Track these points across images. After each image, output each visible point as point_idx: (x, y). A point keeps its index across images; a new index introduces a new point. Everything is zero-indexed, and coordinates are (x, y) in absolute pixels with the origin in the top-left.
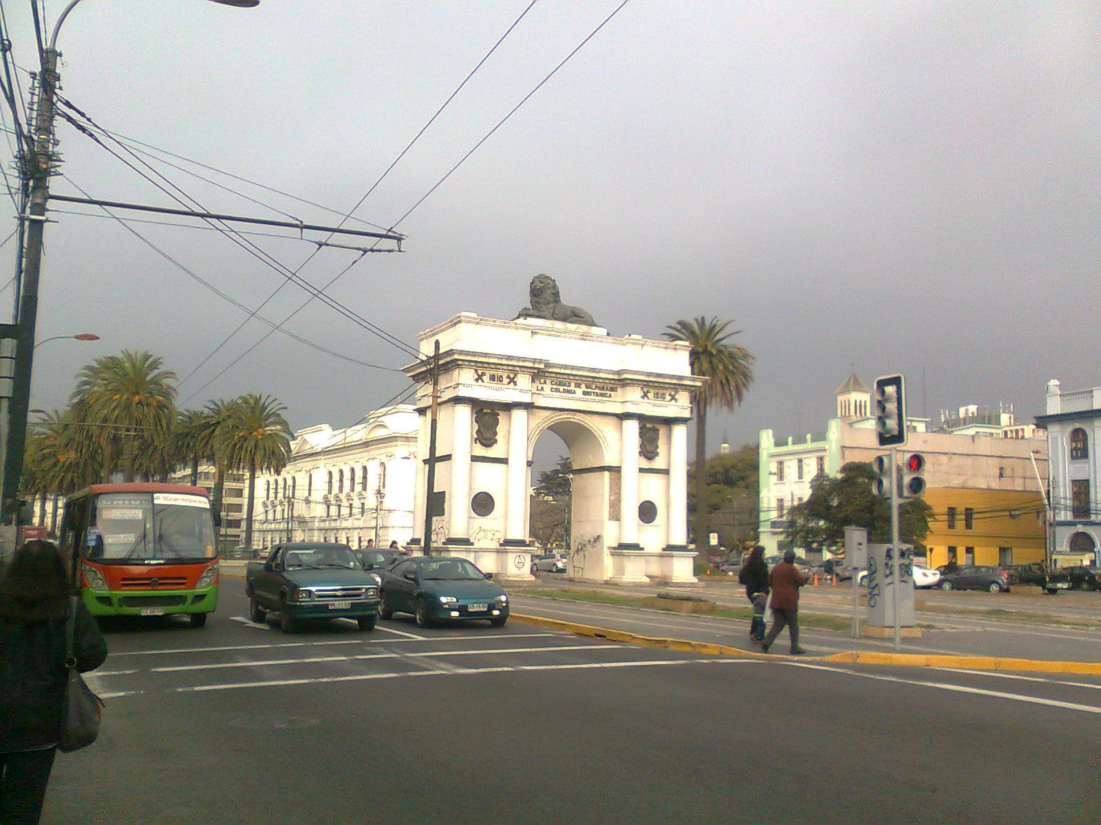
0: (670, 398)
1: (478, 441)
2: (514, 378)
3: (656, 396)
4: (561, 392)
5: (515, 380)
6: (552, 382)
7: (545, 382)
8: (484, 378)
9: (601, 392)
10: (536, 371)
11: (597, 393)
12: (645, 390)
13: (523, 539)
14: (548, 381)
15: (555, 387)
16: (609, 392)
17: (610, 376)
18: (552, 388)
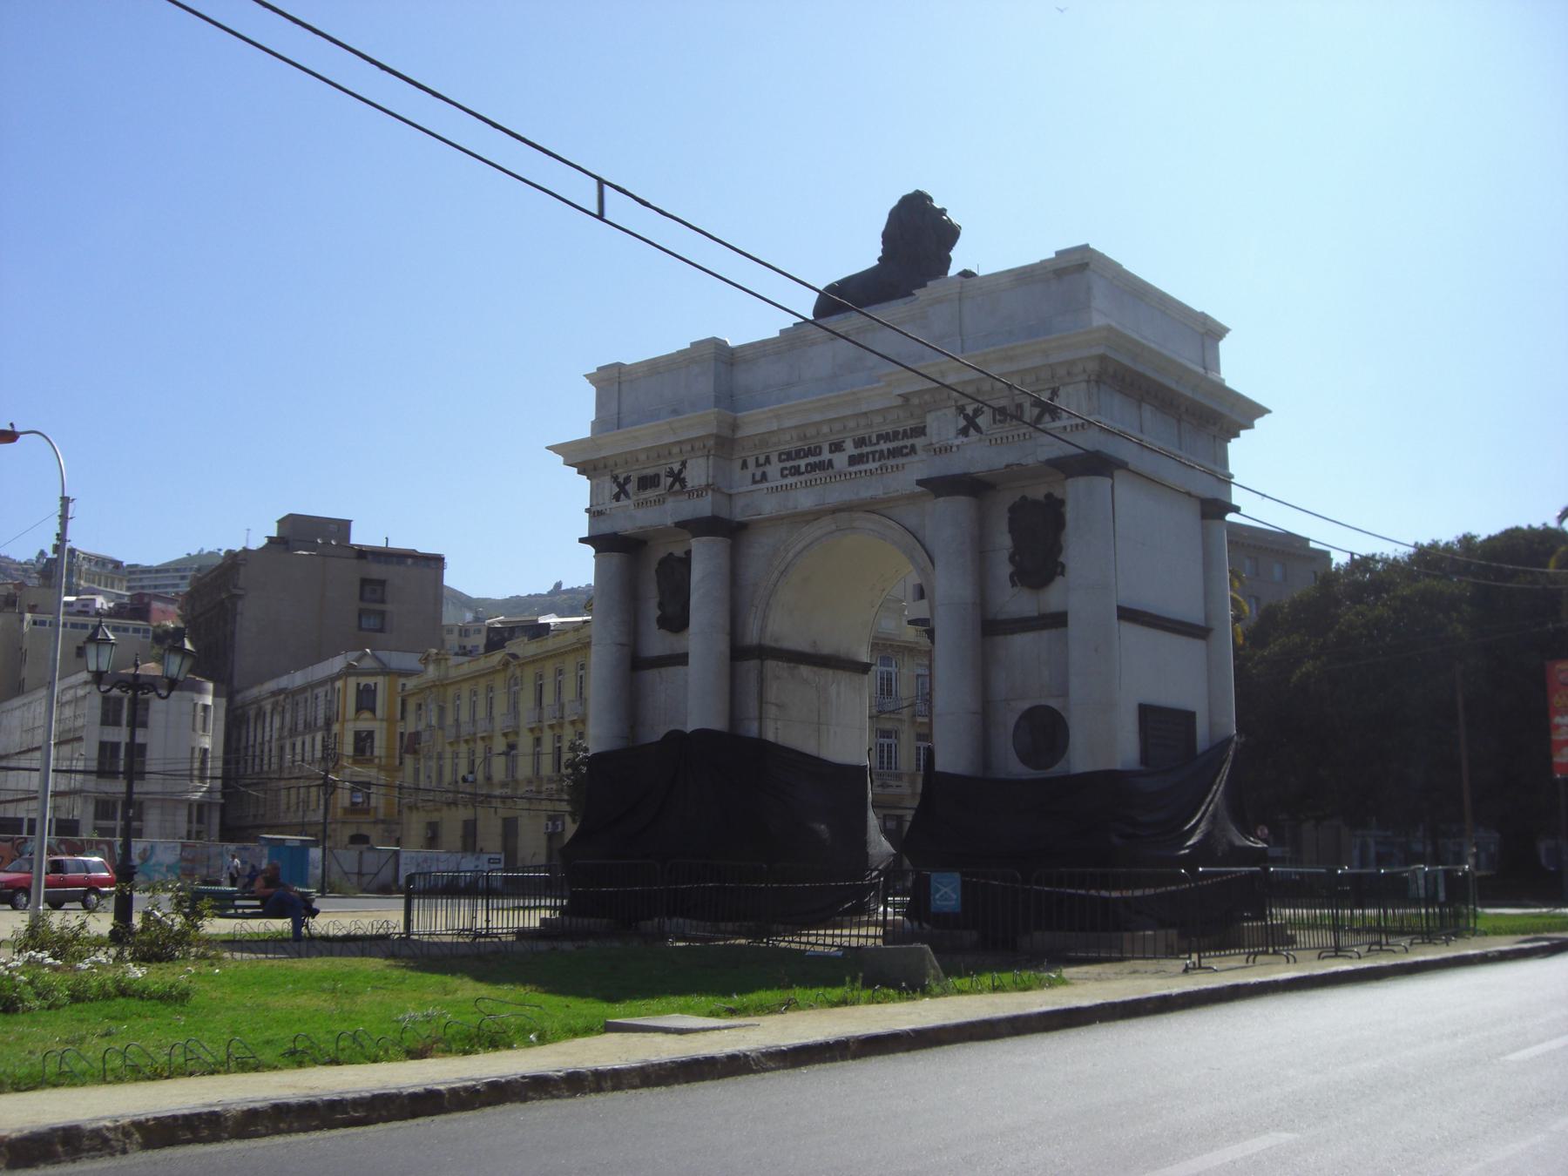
2: (680, 471)
4: (803, 473)
5: (682, 476)
6: (780, 455)
7: (768, 460)
9: (891, 445)
11: (882, 451)
15: (789, 464)
16: (908, 442)
18: (783, 469)
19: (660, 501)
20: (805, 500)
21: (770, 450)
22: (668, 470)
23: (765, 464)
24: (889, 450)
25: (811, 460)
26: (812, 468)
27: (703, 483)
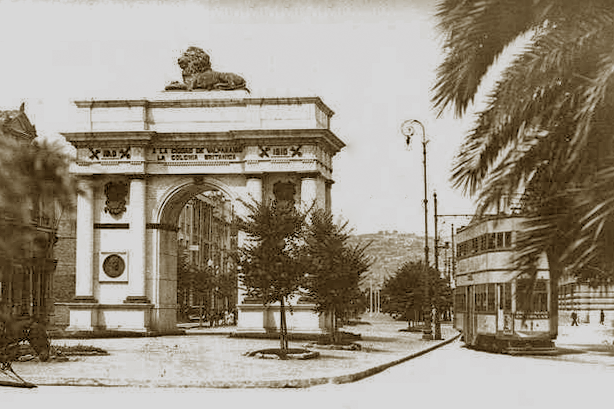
0: (292, 152)
3: (277, 152)
7: (166, 152)
8: (100, 155)
14: (169, 151)
17: (226, 139)
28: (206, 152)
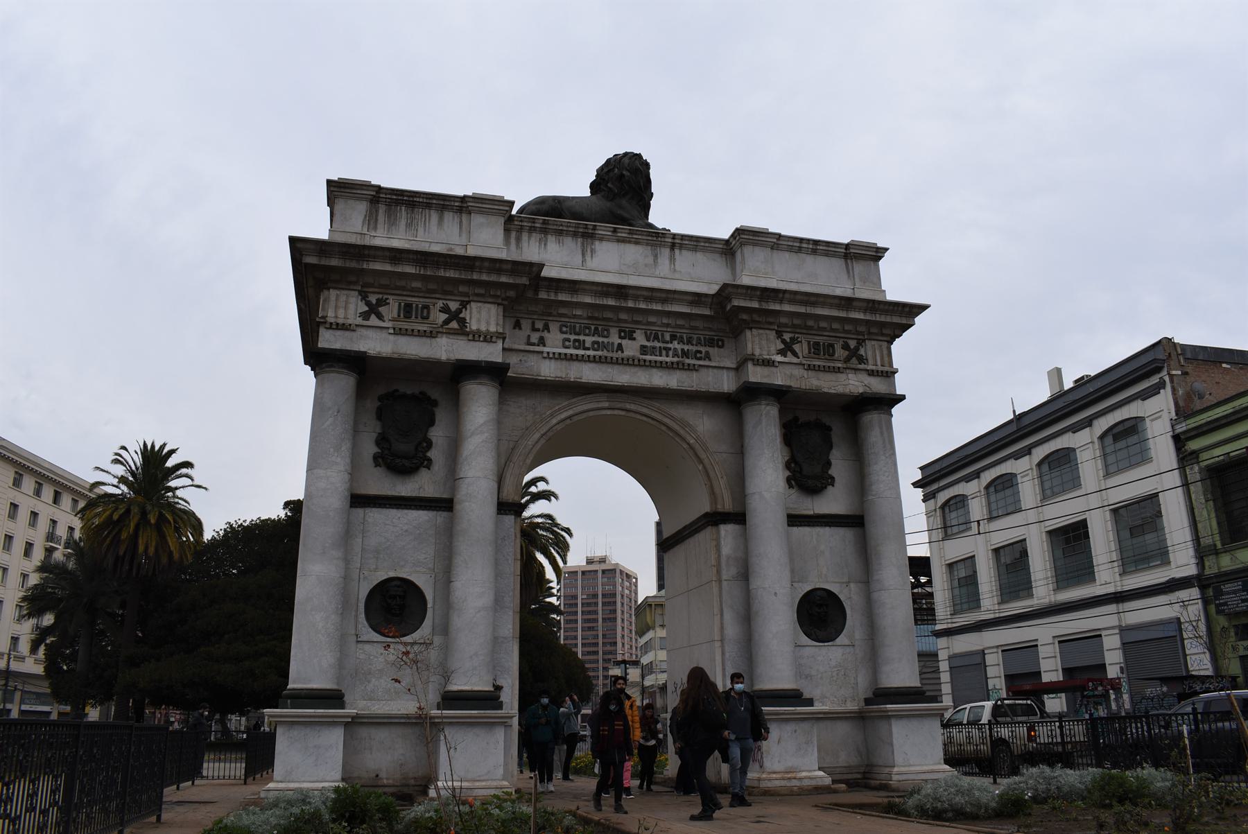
1: (380, 460)
4: (588, 349)
5: (461, 316)
6: (561, 327)
7: (546, 328)
9: (686, 348)
10: (512, 294)
12: (787, 337)
13: (334, 687)
15: (573, 337)
16: (703, 349)
19: (431, 335)
20: (591, 374)
21: (551, 318)
22: (442, 305)
23: (543, 331)
24: (683, 350)
25: (600, 340)
26: (596, 346)
27: (493, 329)
28: (641, 339)
